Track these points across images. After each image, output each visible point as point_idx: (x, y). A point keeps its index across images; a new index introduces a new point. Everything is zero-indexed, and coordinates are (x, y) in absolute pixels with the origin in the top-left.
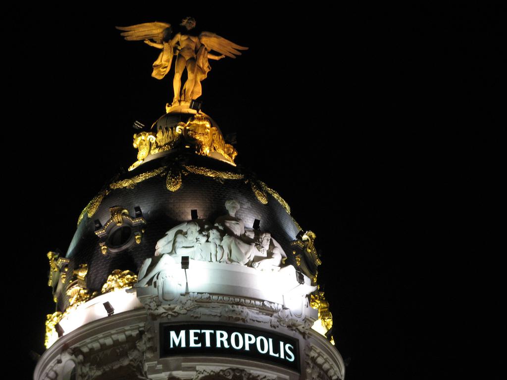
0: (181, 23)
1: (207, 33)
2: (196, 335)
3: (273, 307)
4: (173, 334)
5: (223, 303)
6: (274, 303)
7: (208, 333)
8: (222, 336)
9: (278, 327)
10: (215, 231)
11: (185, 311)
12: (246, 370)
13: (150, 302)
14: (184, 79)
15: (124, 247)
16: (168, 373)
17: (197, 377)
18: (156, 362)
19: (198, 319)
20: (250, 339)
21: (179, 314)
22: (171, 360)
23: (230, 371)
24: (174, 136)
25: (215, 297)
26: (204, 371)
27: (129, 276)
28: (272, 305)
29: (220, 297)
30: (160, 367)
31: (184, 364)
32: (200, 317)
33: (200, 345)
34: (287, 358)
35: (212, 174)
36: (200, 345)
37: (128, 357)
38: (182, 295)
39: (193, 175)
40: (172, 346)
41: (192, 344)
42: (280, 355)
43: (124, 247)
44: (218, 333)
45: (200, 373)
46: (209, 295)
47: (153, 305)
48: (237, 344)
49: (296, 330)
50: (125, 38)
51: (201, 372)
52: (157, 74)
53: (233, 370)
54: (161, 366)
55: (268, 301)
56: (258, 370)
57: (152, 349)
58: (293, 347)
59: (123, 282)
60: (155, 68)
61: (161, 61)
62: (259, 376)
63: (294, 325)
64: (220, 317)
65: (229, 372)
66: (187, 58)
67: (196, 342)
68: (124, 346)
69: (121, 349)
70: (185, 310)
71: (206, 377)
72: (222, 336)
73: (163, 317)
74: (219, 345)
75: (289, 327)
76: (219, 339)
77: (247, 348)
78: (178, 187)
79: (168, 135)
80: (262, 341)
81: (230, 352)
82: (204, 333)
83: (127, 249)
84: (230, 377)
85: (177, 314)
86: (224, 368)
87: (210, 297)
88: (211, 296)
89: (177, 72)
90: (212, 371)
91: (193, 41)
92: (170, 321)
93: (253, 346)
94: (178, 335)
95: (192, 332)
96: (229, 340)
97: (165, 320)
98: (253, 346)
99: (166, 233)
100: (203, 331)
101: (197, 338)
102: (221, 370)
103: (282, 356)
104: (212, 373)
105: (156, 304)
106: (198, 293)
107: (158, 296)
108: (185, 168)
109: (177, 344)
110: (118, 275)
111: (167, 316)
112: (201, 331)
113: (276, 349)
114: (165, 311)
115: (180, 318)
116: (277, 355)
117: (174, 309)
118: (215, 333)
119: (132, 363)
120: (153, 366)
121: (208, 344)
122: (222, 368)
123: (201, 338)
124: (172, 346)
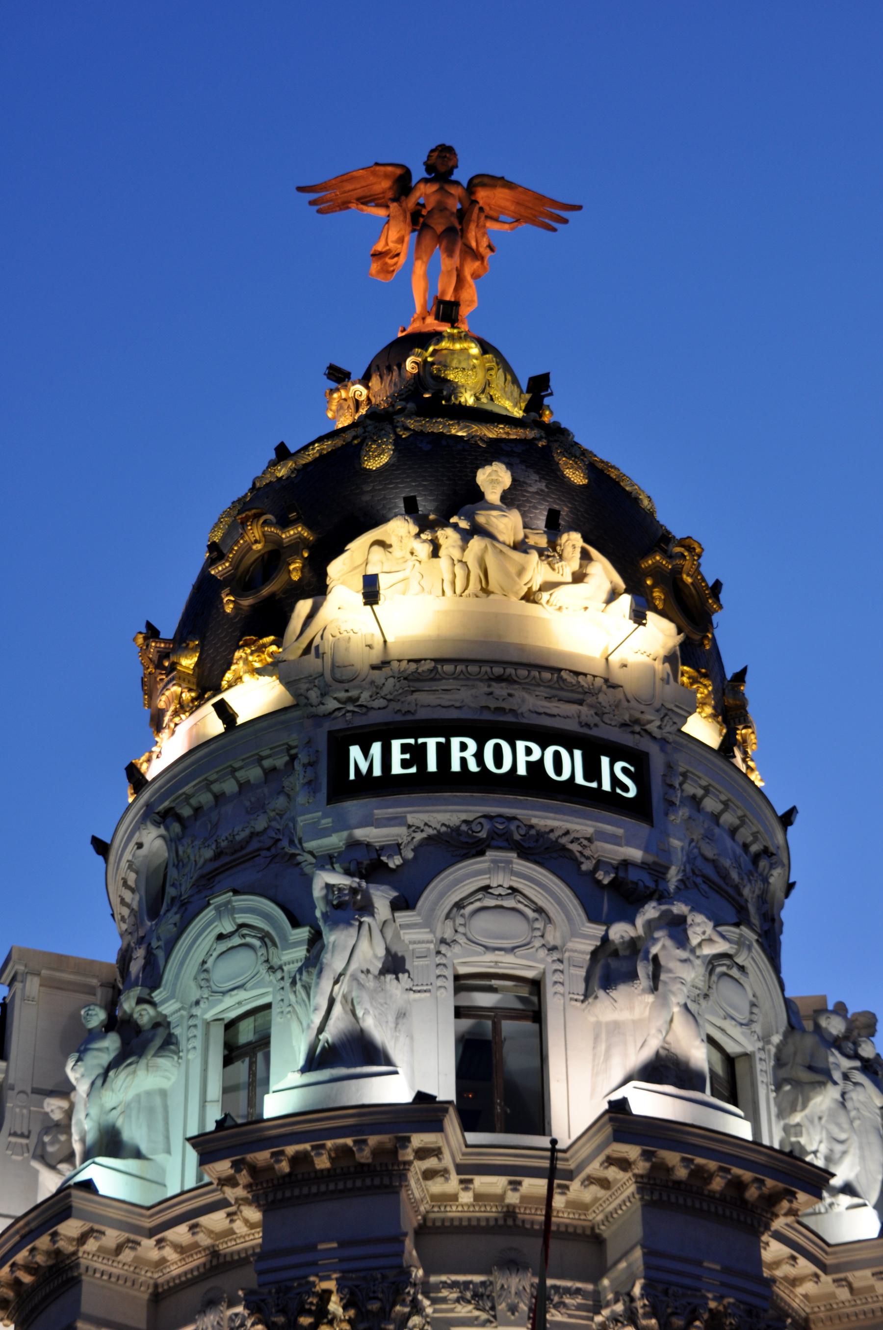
2: (405, 748)
3: (583, 683)
4: (355, 752)
5: (468, 679)
6: (585, 675)
7: (431, 743)
8: (464, 747)
9: (596, 725)
10: (449, 531)
11: (382, 703)
12: (519, 817)
13: (308, 690)
15: (266, 591)
16: (345, 834)
17: (409, 839)
18: (320, 814)
19: (409, 717)
21: (369, 709)
22: (353, 807)
23: (482, 820)
25: (448, 668)
26: (426, 824)
27: (273, 648)
28: (581, 678)
30: (327, 822)
31: (379, 813)
32: (416, 711)
33: (413, 770)
34: (618, 791)
35: (461, 429)
36: (413, 770)
38: (374, 667)
40: (352, 776)
41: (397, 769)
43: (266, 591)
44: (455, 742)
45: (418, 829)
46: (433, 664)
49: (643, 733)
51: (418, 828)
54: (329, 820)
55: (571, 671)
58: (632, 769)
59: (260, 661)
61: (387, 244)
62: (552, 831)
63: (637, 722)
65: (480, 823)
66: (440, 229)
67: (405, 764)
70: (382, 700)
71: (430, 838)
72: (464, 747)
73: (336, 718)
74: (456, 767)
75: (624, 725)
77: (522, 770)
78: (385, 459)
80: (557, 756)
83: (272, 595)
84: (483, 835)
85: (364, 710)
86: (470, 817)
87: (435, 668)
88: (439, 667)
90: (443, 825)
91: (451, 194)
92: (350, 726)
93: (536, 767)
94: (366, 752)
95: (396, 745)
96: (479, 756)
97: (339, 725)
98: (536, 767)
99: (346, 548)
100: (420, 741)
101: (407, 756)
103: (606, 786)
104: (444, 829)
105: (319, 693)
106: (409, 661)
107: (322, 675)
110: (250, 648)
111: (344, 715)
112: (416, 742)
113: (592, 771)
114: (337, 705)
116: (594, 785)
117: (358, 699)
118: (448, 743)
120: (315, 823)
121: (432, 766)
122: (464, 816)
123: (417, 755)
124: (352, 776)
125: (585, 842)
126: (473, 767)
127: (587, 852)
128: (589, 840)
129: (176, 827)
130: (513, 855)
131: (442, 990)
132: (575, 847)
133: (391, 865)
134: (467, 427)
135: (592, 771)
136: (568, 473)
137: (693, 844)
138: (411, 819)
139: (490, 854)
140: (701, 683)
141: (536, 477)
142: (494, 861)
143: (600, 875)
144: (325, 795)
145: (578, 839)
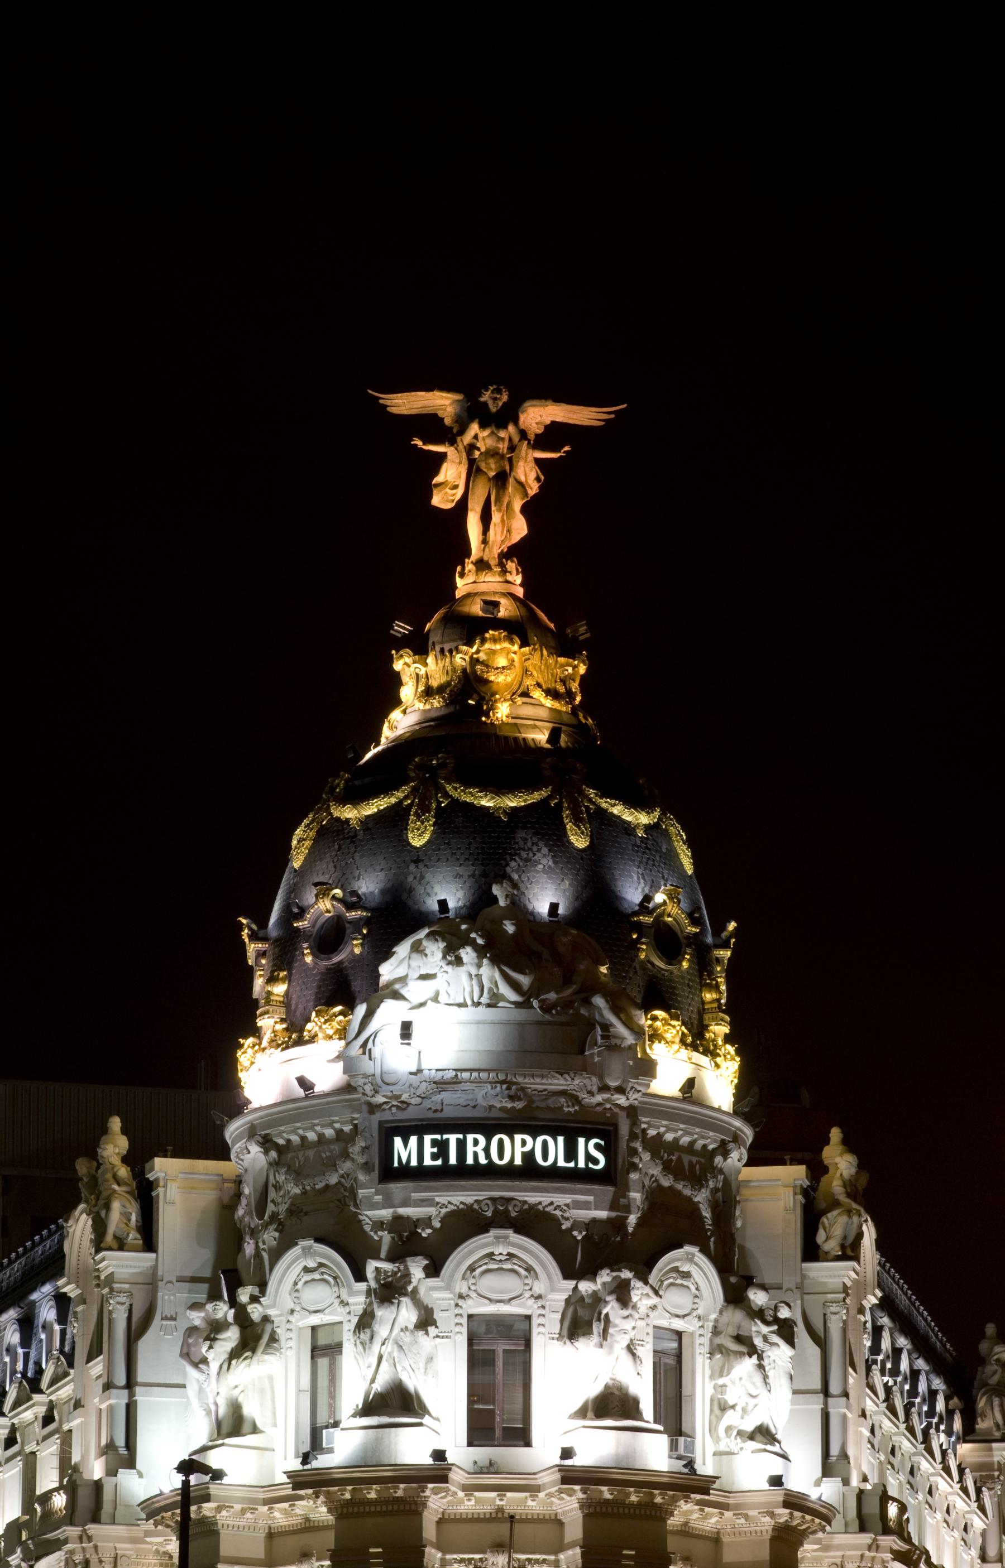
0: (480, 396)
1: (535, 402)
2: (434, 1143)
4: (398, 1141)
5: (480, 1082)
7: (453, 1139)
8: (476, 1142)
10: (469, 949)
11: (418, 1100)
13: (365, 1084)
14: (486, 519)
15: (336, 959)
16: (391, 1210)
19: (438, 1115)
20: (524, 1143)
21: (408, 1104)
22: (397, 1188)
23: (489, 1202)
24: (454, 670)
25: (466, 1075)
26: (449, 1203)
27: (341, 1018)
29: (475, 1074)
30: (378, 1198)
32: (442, 1110)
33: (439, 1162)
34: (591, 1165)
36: (439, 1162)
37: (337, 1170)
38: (411, 1073)
39: (456, 804)
40: (396, 1164)
42: (576, 1164)
43: (336, 959)
44: (470, 1138)
45: (444, 1206)
46: (454, 1073)
47: (368, 1088)
48: (501, 1156)
50: (388, 409)
51: (443, 1205)
52: (440, 502)
53: (493, 1200)
54: (381, 1197)
56: (536, 1196)
57: (367, 1167)
58: (603, 1143)
59: (332, 1028)
60: (435, 492)
62: (540, 1203)
64: (474, 1107)
65: (487, 1204)
66: (492, 474)
67: (434, 1157)
68: (332, 1147)
69: (328, 1154)
70: (418, 1098)
71: (452, 1212)
72: (476, 1142)
73: (384, 1110)
74: (470, 1160)
76: (470, 1149)
77: (518, 1161)
78: (427, 837)
79: (444, 666)
81: (489, 1172)
82: (448, 1140)
83: (341, 962)
84: (489, 1214)
85: (405, 1105)
86: (481, 1198)
87: (457, 1075)
88: (459, 1074)
89: (471, 510)
90: (462, 1203)
92: (395, 1118)
94: (406, 1143)
95: (428, 1139)
96: (487, 1150)
97: (387, 1116)
100: (445, 1136)
101: (435, 1150)
102: (476, 1201)
103: (581, 1164)
104: (461, 1206)
105: (372, 1088)
106: (437, 1070)
107: (374, 1075)
108: (444, 788)
109: (404, 1161)
110: (323, 1017)
111: (390, 1108)
112: (442, 1137)
113: (571, 1154)
114: (385, 1100)
115: (411, 1114)
116: (572, 1165)
117: (400, 1096)
118: (465, 1138)
119: (343, 1180)
120: (369, 1196)
121: (453, 1160)
122: (476, 1198)
123: (442, 1148)
124: (396, 1164)
125: (565, 1208)
126: (483, 1160)
127: (565, 1215)
128: (567, 1205)
129: (273, 1154)
130: (510, 1232)
131: (459, 1335)
132: (558, 1213)
133: (424, 1235)
134: (493, 798)
135: (571, 1154)
136: (573, 839)
137: (654, 1179)
138: (437, 1199)
139: (494, 1232)
140: (670, 1025)
141: (545, 850)
142: (496, 1238)
143: (575, 1233)
144: (377, 1175)
145: (559, 1206)
